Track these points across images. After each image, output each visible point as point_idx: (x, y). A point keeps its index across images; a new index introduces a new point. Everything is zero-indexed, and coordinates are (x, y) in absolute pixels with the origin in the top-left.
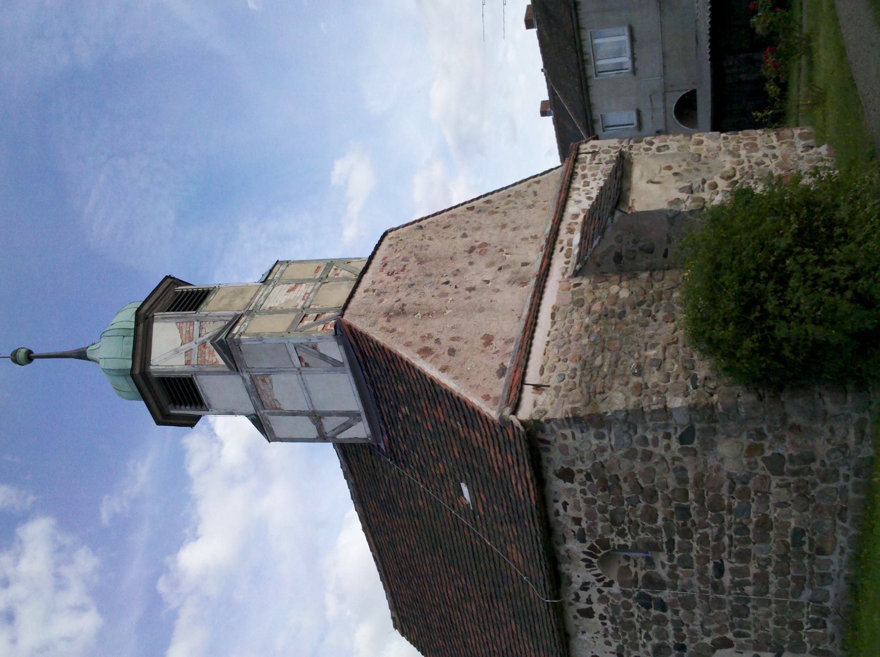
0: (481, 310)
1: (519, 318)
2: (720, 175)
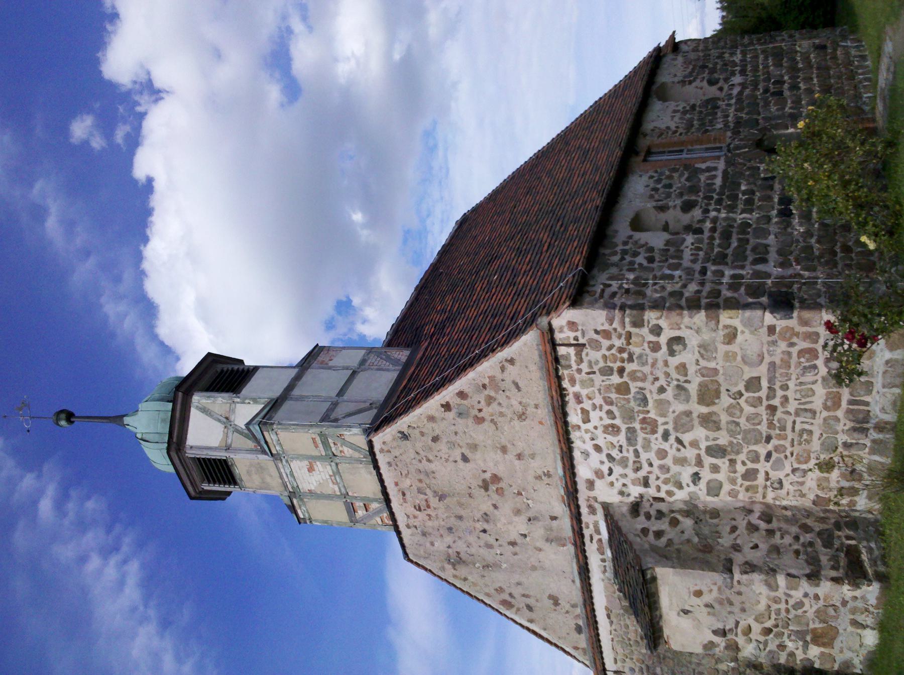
0: (534, 568)
1: (573, 581)
2: (753, 617)
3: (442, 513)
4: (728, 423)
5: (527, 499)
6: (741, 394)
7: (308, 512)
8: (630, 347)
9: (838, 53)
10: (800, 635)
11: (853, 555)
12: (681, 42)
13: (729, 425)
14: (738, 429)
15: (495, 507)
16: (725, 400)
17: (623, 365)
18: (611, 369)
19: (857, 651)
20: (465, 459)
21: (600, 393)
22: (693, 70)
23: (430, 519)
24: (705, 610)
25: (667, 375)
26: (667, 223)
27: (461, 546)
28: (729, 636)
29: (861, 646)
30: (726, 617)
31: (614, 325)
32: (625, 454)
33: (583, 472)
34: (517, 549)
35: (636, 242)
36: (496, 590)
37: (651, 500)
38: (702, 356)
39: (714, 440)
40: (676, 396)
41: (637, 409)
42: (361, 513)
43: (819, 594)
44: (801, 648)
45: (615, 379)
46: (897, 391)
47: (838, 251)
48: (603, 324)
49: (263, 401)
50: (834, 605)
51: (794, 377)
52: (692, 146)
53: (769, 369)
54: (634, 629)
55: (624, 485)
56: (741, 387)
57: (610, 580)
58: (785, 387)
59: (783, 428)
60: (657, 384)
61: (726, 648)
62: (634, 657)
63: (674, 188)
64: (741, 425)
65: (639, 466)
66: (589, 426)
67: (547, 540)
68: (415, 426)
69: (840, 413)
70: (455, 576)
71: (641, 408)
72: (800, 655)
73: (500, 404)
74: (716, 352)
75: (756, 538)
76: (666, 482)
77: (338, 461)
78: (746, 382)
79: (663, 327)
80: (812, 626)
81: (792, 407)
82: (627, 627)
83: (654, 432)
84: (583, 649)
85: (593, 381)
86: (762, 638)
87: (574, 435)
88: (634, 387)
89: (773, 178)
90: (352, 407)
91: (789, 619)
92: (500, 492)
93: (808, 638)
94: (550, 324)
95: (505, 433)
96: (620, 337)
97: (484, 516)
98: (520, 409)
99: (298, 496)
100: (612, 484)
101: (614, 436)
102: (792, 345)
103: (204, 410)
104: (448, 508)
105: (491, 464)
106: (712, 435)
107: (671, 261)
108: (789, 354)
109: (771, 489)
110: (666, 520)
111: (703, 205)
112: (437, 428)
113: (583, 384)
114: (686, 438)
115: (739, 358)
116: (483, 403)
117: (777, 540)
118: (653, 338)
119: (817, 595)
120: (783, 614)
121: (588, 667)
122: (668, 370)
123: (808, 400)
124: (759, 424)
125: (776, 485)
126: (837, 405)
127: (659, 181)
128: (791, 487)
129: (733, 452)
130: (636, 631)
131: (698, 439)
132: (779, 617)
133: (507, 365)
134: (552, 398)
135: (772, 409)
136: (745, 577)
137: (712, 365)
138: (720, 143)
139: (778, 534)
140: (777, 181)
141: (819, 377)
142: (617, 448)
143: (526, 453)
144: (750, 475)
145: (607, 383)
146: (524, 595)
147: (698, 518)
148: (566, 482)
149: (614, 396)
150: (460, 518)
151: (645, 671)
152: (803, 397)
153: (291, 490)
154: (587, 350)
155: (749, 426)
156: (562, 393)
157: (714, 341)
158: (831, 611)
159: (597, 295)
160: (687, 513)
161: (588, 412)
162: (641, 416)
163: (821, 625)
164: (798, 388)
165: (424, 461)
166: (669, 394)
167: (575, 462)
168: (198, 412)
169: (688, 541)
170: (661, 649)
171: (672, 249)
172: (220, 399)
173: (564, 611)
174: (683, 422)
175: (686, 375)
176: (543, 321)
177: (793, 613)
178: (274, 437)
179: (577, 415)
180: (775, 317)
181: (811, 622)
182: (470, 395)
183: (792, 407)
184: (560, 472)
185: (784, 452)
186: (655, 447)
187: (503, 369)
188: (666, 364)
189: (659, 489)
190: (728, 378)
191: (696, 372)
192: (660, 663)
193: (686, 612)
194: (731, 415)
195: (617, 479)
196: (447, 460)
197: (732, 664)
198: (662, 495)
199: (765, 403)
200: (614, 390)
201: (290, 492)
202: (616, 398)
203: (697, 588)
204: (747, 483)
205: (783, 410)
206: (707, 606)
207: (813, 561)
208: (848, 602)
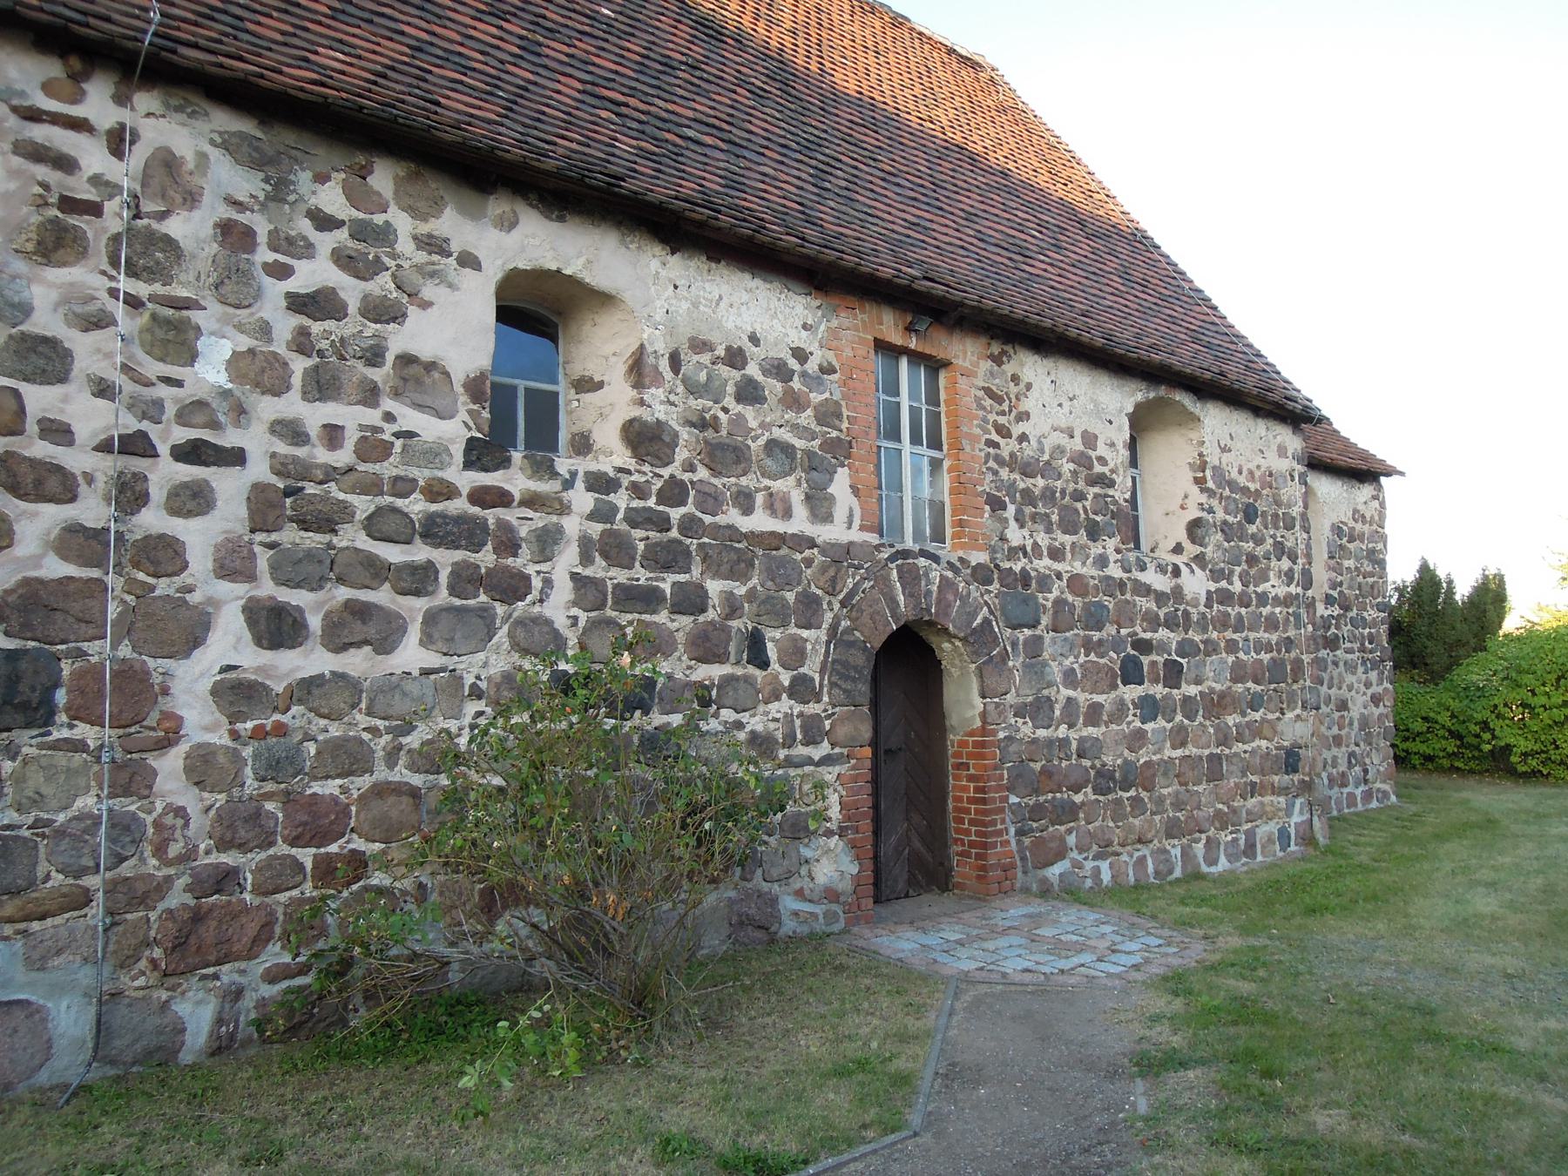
9: (1268, 799)
12: (1380, 488)
22: (1245, 490)
26: (600, 385)
63: (736, 408)
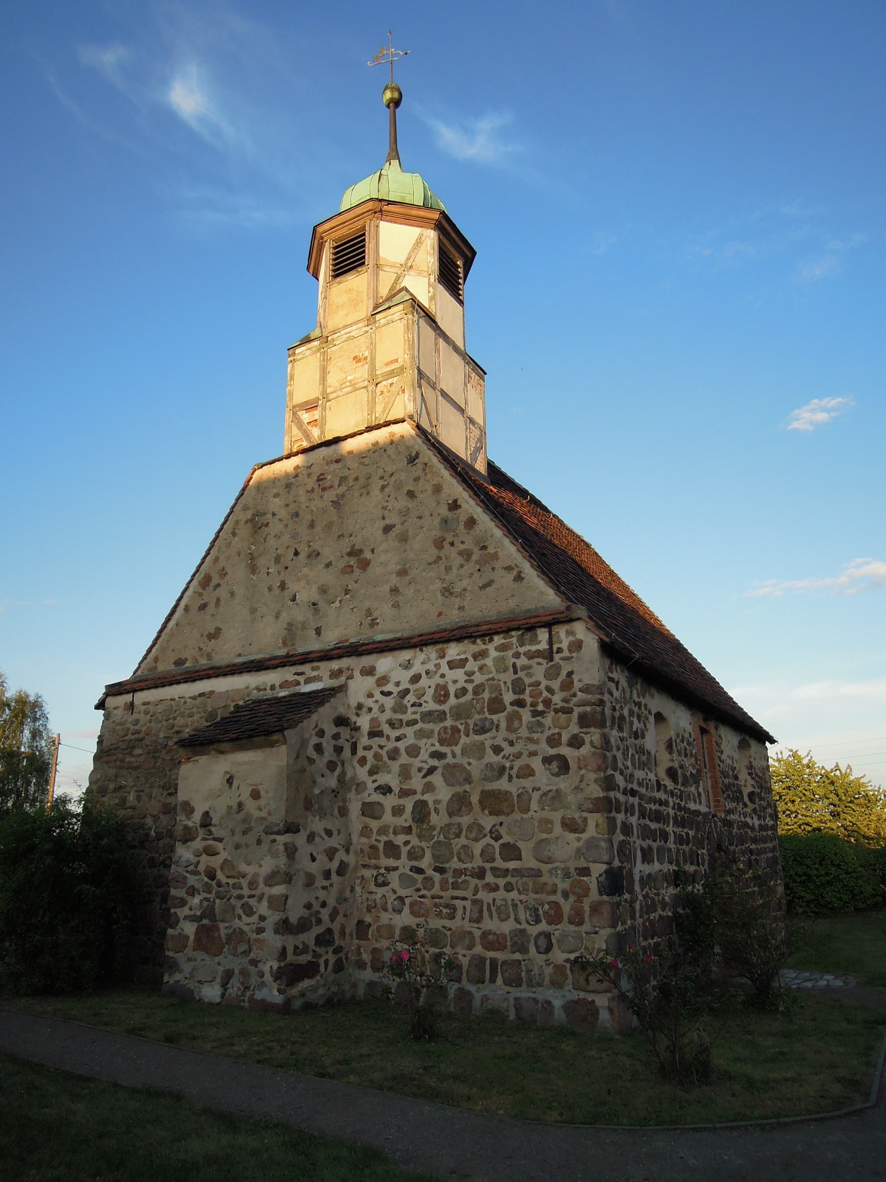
0: (253, 611)
1: (240, 655)
2: (229, 858)
3: (317, 504)
4: (459, 824)
5: (340, 601)
6: (496, 839)
7: (303, 358)
8: (552, 713)
10: (209, 912)
11: (310, 970)
13: (456, 826)
14: (452, 836)
15: (328, 565)
16: (488, 822)
17: (528, 705)
18: (522, 691)
19: (192, 976)
20: (387, 529)
21: (489, 679)
23: (308, 492)
24: (234, 803)
25: (518, 756)
27: (275, 527)
28: (201, 832)
29: (200, 982)
30: (227, 827)
31: (579, 693)
32: (410, 710)
33: (384, 663)
34: (276, 591)
35: (647, 719)
36: (223, 569)
37: (354, 740)
38: (545, 794)
39: (436, 809)
40: (489, 766)
41: (471, 722)
42: (305, 417)
43: (264, 934)
44: (192, 913)
45: (508, 697)
46: (512, 1016)
47: (655, 940)
48: (580, 681)
49: (433, 307)
50: (250, 951)
51: (523, 897)
52: (710, 778)
53: (532, 869)
54: (189, 725)
55: (370, 710)
56: (506, 839)
57: (249, 695)
58: (509, 888)
59: (455, 886)
60: (505, 745)
61: (186, 827)
62: (153, 724)
64: (457, 839)
65: (396, 726)
66: (445, 668)
67: (290, 624)
68: (427, 471)
69: (478, 949)
70: (237, 522)
71: (471, 727)
72: (183, 912)
73: (462, 566)
74: (551, 810)
75: (322, 858)
76: (377, 756)
77: (370, 388)
78: (514, 844)
79: (581, 749)
80: (222, 926)
81: (482, 895)
82: (191, 715)
83: (442, 742)
84: (156, 668)
85: (505, 671)
86: (201, 868)
87: (431, 652)
88: (500, 718)
89: (698, 865)
90: (431, 405)
91: (229, 900)
92: (348, 570)
93: (205, 922)
94: (579, 619)
95: (424, 574)
96: (565, 700)
97: (315, 553)
98: (457, 589)
99: (323, 346)
100: (370, 695)
101: (433, 696)
102: (566, 895)
103: (419, 242)
104: (324, 511)
105: (383, 558)
106: (443, 807)
107: (637, 757)
108: (554, 892)
109: (375, 874)
110: (334, 758)
111: (676, 791)
112: (426, 497)
113: (499, 661)
114: (437, 779)
115: (544, 836)
116: (462, 547)
117: (320, 882)
118: (565, 738)
119: (263, 932)
120: (236, 893)
121: (135, 673)
122: (524, 756)
123: (494, 913)
124: (460, 860)
125: (381, 879)
126: (489, 946)
127: (689, 744)
128: (379, 896)
129: (421, 831)
130: (187, 726)
131: (436, 791)
132: (231, 888)
133: (515, 573)
134: (478, 626)
135: (480, 874)
136: (282, 848)
137: (534, 806)
138: (715, 806)
139: (326, 883)
140: (697, 868)
141: (524, 925)
142: (418, 701)
143: (401, 597)
144: (392, 850)
145: (503, 688)
146: (218, 600)
147: (338, 793)
148: (367, 644)
149: (486, 695)
150: (312, 525)
151: (136, 736)
152: (498, 908)
153: (329, 338)
154: (545, 663)
155: (456, 849)
156: (488, 635)
157: (566, 807)
158: (242, 948)
159: (610, 675)
160: (341, 779)
161: (463, 667)
162: (462, 728)
163: (223, 936)
164: (510, 903)
165: (382, 482)
166: (491, 758)
167: (397, 653)
168: (416, 236)
169: (314, 782)
170: (182, 753)
171: (644, 758)
172: (432, 260)
173: (202, 645)
174: (454, 773)
175: (518, 777)
176: (581, 611)
177: (239, 904)
178: (396, 317)
179: (458, 654)
180: (601, 875)
181: (227, 925)
182: (471, 532)
183: (482, 895)
184: (379, 637)
185: (425, 888)
186: (422, 743)
187: (509, 569)
188: (533, 754)
189: (367, 748)
190: (517, 824)
191: (524, 788)
192: (149, 753)
193: (230, 781)
194: (470, 828)
195: (377, 701)
196: (384, 508)
197: (153, 833)
198: (360, 753)
199: (487, 866)
200: (493, 695)
201: (328, 337)
202: (483, 698)
203: (263, 793)
204: (381, 846)
205: (480, 886)
206: (240, 805)
207: (303, 926)
208: (256, 967)
